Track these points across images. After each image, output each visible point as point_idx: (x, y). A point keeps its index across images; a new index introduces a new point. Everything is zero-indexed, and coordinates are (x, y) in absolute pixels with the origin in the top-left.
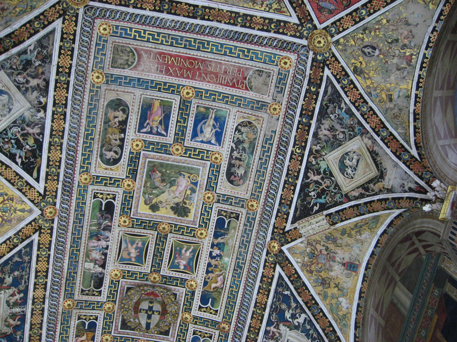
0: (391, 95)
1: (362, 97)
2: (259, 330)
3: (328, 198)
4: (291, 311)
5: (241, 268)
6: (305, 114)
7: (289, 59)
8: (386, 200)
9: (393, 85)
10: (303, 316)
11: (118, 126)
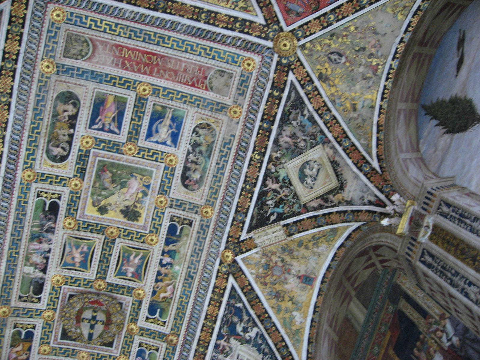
0: (355, 104)
1: (326, 105)
2: (209, 343)
3: (286, 207)
4: (243, 325)
5: (192, 277)
6: (266, 119)
7: (253, 61)
8: (345, 212)
9: (357, 94)
10: (255, 330)
11: (68, 121)
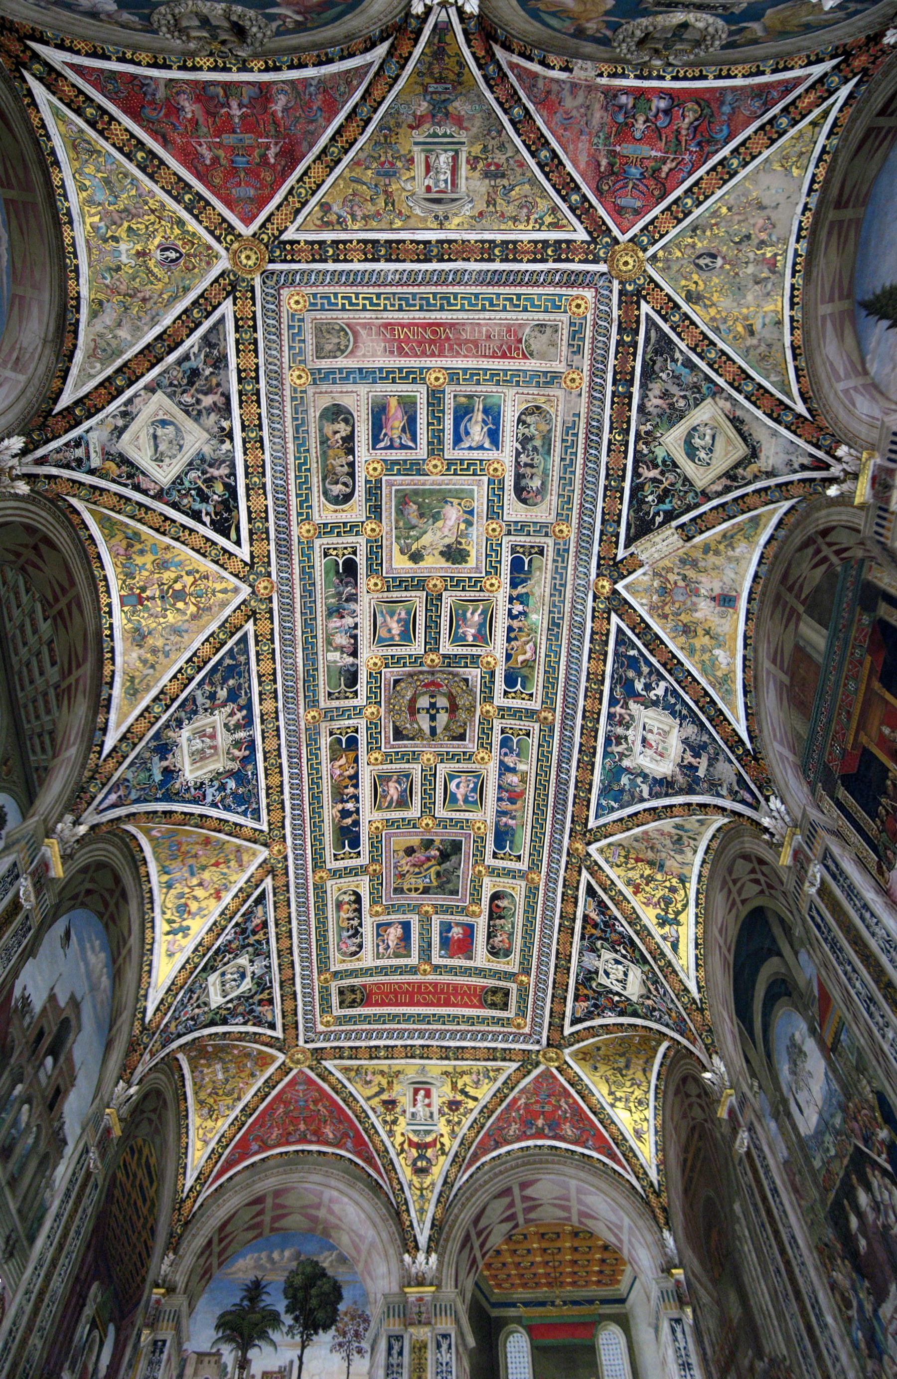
5: (558, 625)
8: (766, 489)
